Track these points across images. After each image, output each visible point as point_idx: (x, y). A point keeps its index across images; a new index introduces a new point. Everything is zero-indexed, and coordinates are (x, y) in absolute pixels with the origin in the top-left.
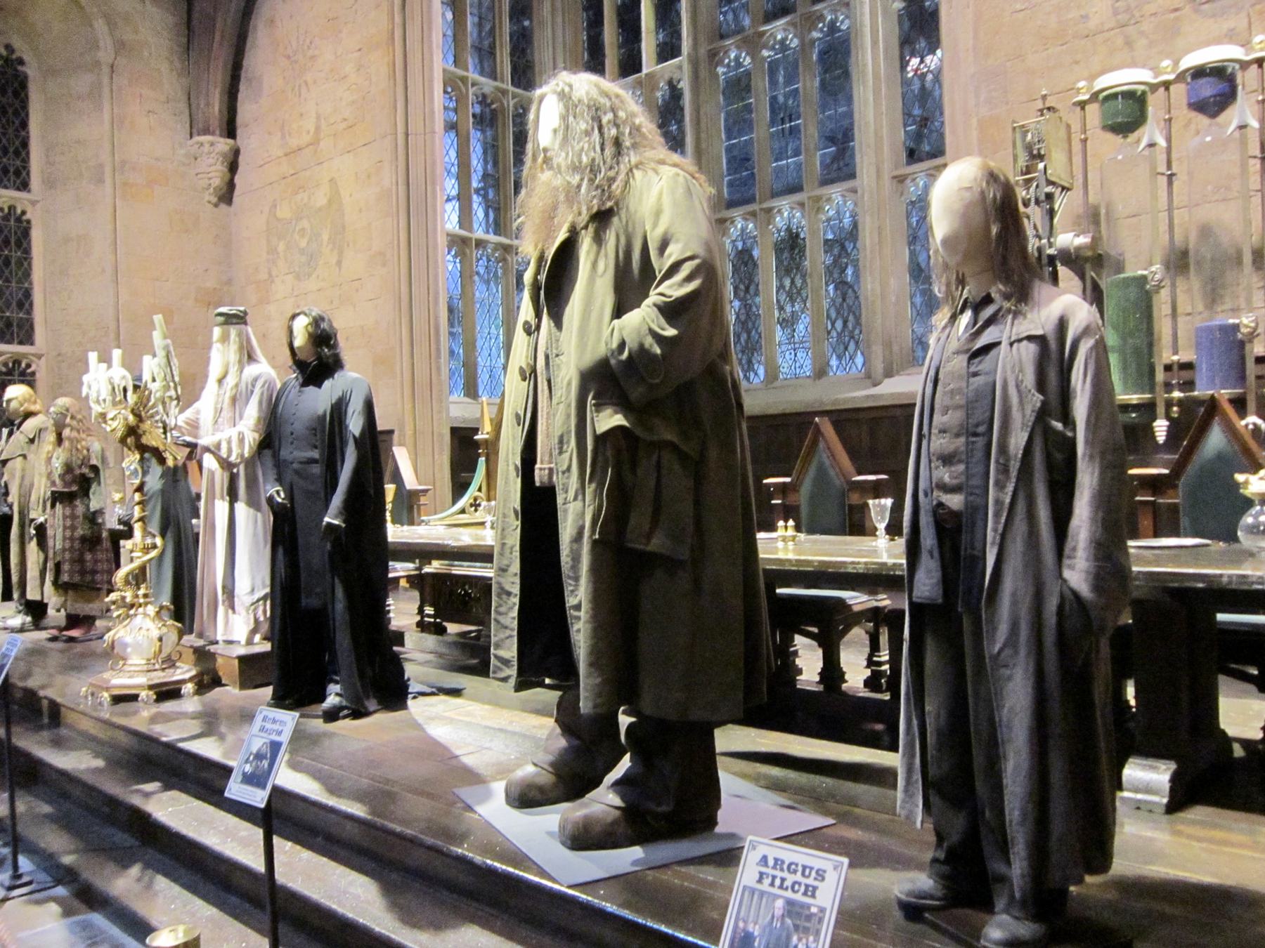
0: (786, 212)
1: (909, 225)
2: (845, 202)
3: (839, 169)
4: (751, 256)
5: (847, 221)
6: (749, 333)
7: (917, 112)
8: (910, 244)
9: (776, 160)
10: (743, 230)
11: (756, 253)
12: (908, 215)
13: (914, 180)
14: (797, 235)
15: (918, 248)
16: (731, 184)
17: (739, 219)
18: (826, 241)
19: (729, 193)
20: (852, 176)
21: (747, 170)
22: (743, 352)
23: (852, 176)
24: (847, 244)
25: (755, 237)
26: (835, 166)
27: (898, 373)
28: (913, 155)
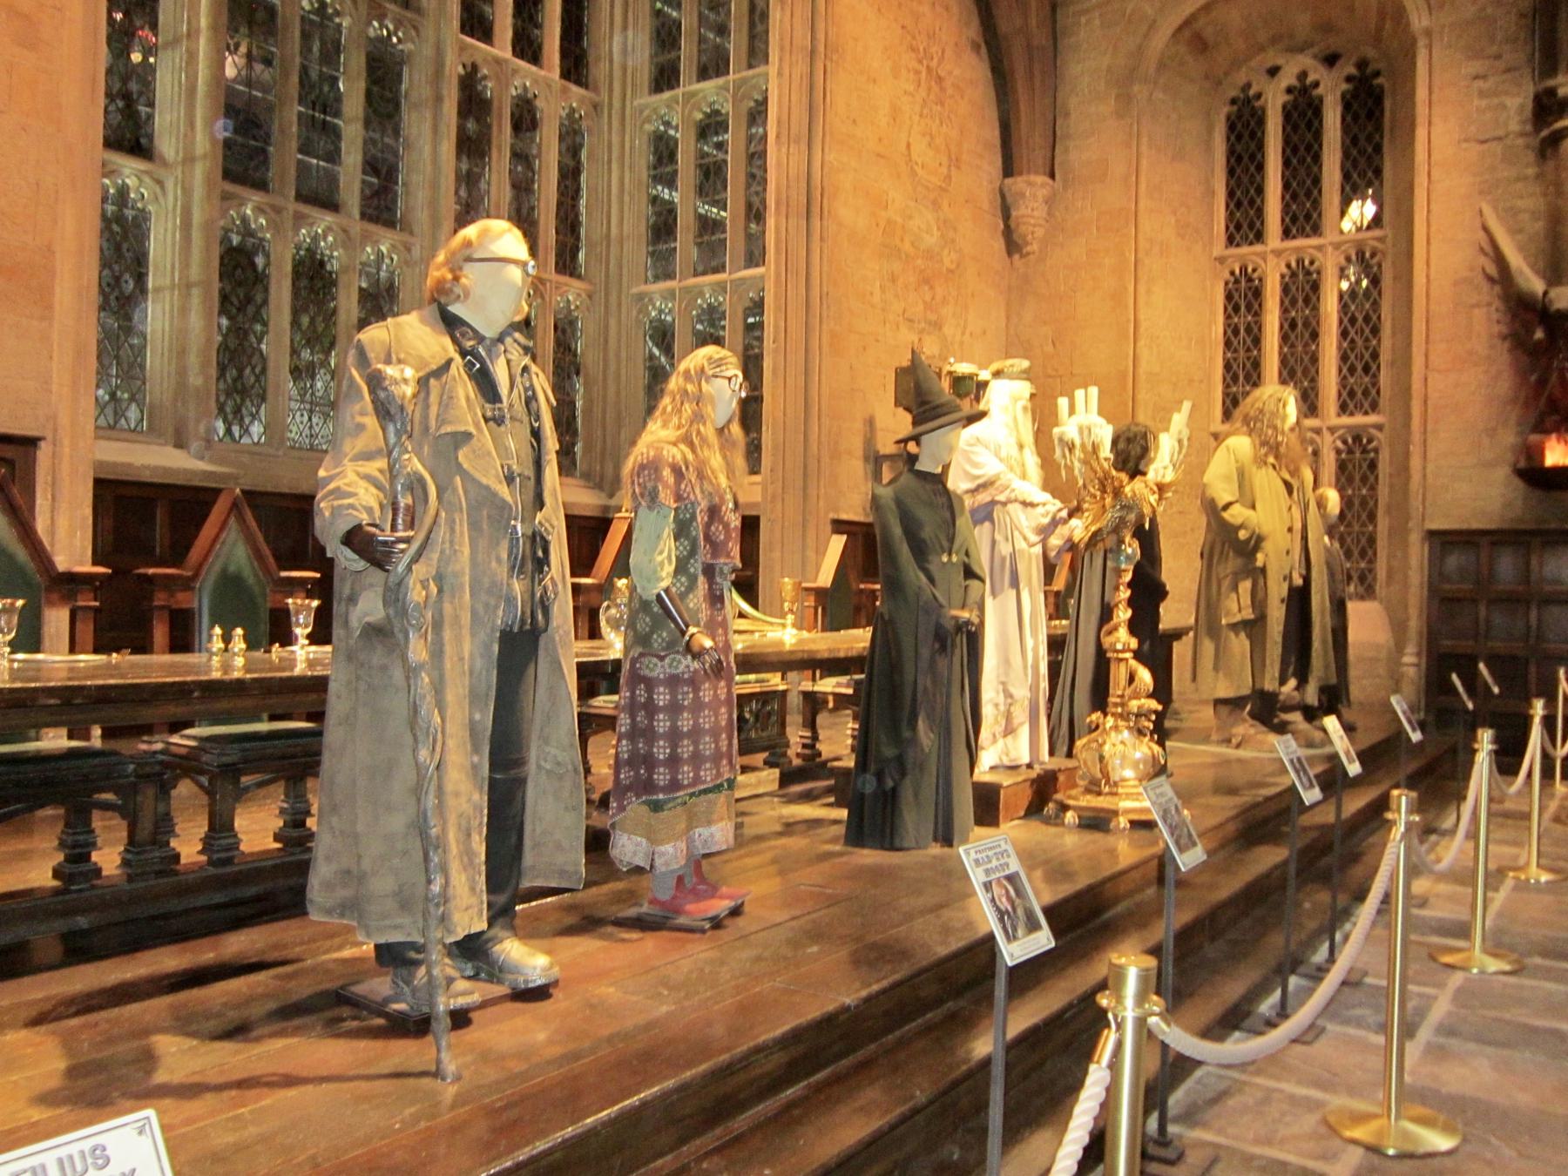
0: (322, 230)
4: (253, 265)
6: (241, 371)
7: (463, 193)
11: (260, 261)
14: (322, 264)
18: (361, 289)
21: (254, 138)
22: (228, 394)
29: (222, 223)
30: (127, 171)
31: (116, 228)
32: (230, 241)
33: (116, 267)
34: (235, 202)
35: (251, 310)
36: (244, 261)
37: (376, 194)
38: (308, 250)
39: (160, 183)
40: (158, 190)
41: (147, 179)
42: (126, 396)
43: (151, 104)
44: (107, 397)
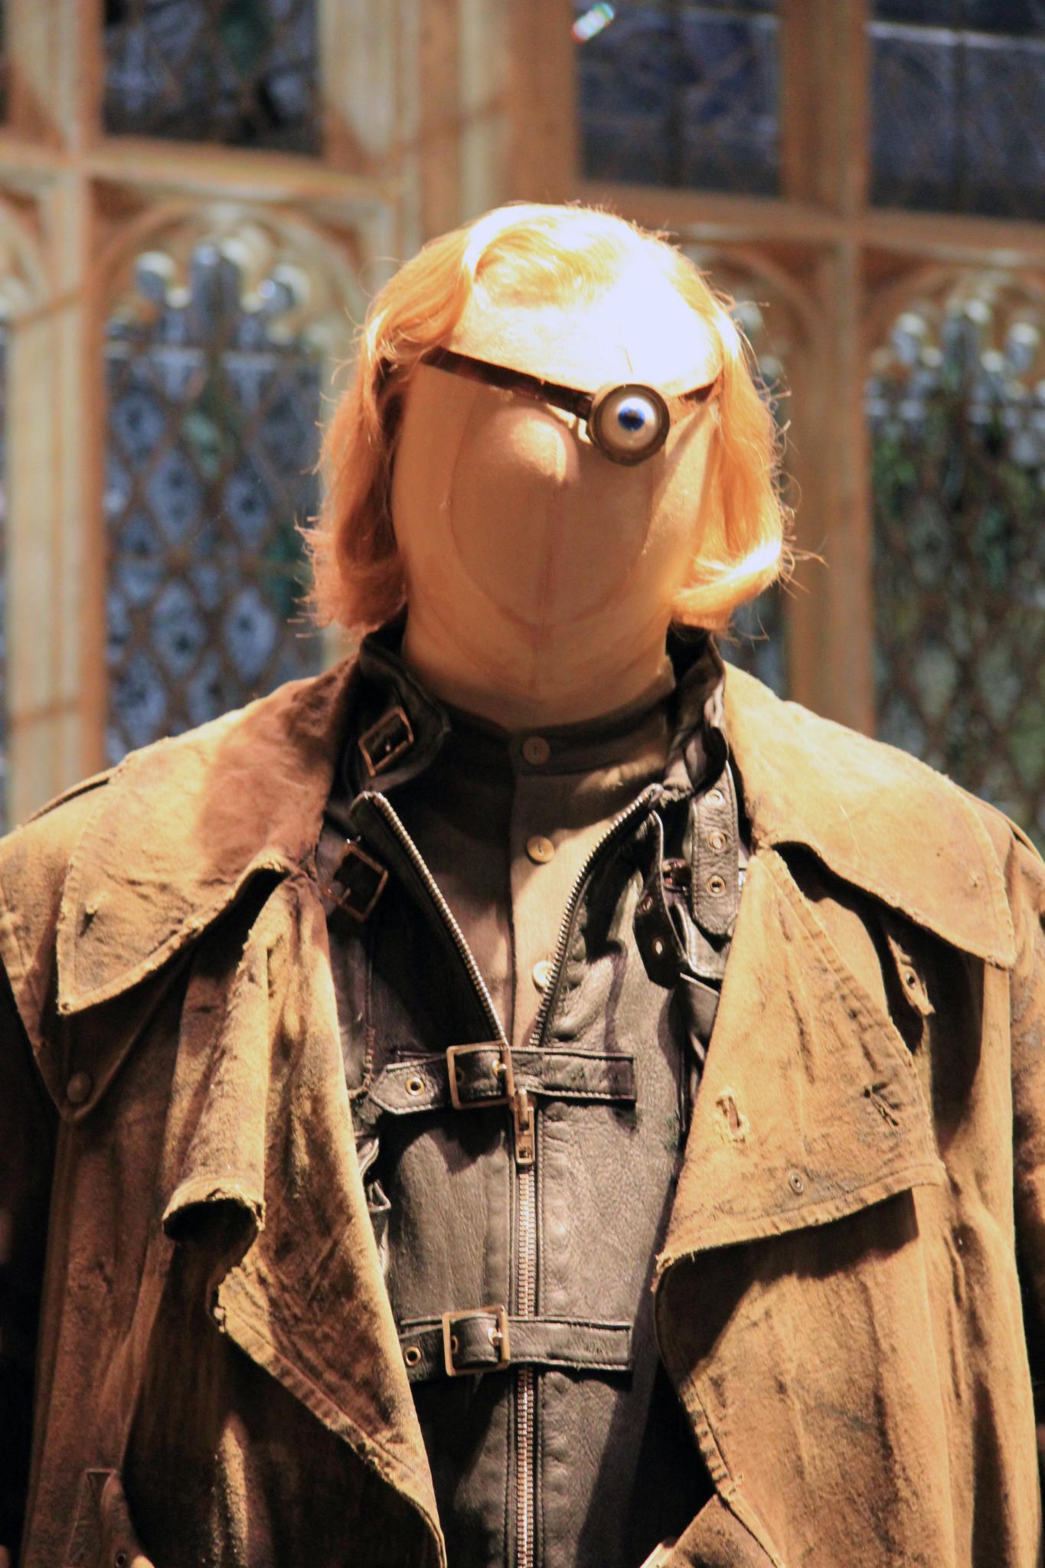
30: (224, 215)
33: (207, 576)
38: (935, 395)
40: (336, 258)
41: (299, 232)
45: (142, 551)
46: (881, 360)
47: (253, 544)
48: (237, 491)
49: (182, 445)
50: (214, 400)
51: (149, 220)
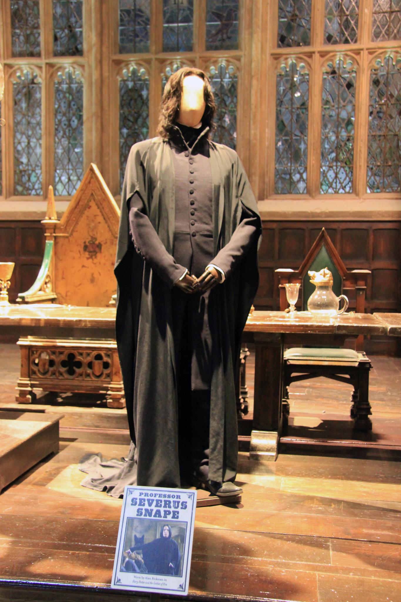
1: (278, 92)
2: (228, 65)
3: (223, 40)
4: (141, 96)
5: (226, 80)
8: (277, 105)
9: (168, 22)
10: (134, 72)
11: (144, 93)
12: (278, 85)
13: (286, 59)
15: (283, 110)
16: (122, 33)
17: (133, 63)
19: (122, 40)
20: (236, 47)
21: (139, 24)
23: (236, 47)
24: (226, 98)
25: (145, 80)
26: (220, 36)
27: (267, 198)
28: (283, 41)
29: (120, 79)
31: (67, 95)
32: (127, 86)
34: (123, 65)
35: (140, 121)
36: (136, 96)
37: (220, 31)
39: (83, 66)
40: (81, 69)
41: (76, 66)
42: (75, 178)
43: (81, 27)
44: (67, 180)
45: (60, 112)
46: (162, 74)
47: (75, 110)
48: (73, 103)
49: (65, 97)
50: (70, 90)
51: (56, 68)
